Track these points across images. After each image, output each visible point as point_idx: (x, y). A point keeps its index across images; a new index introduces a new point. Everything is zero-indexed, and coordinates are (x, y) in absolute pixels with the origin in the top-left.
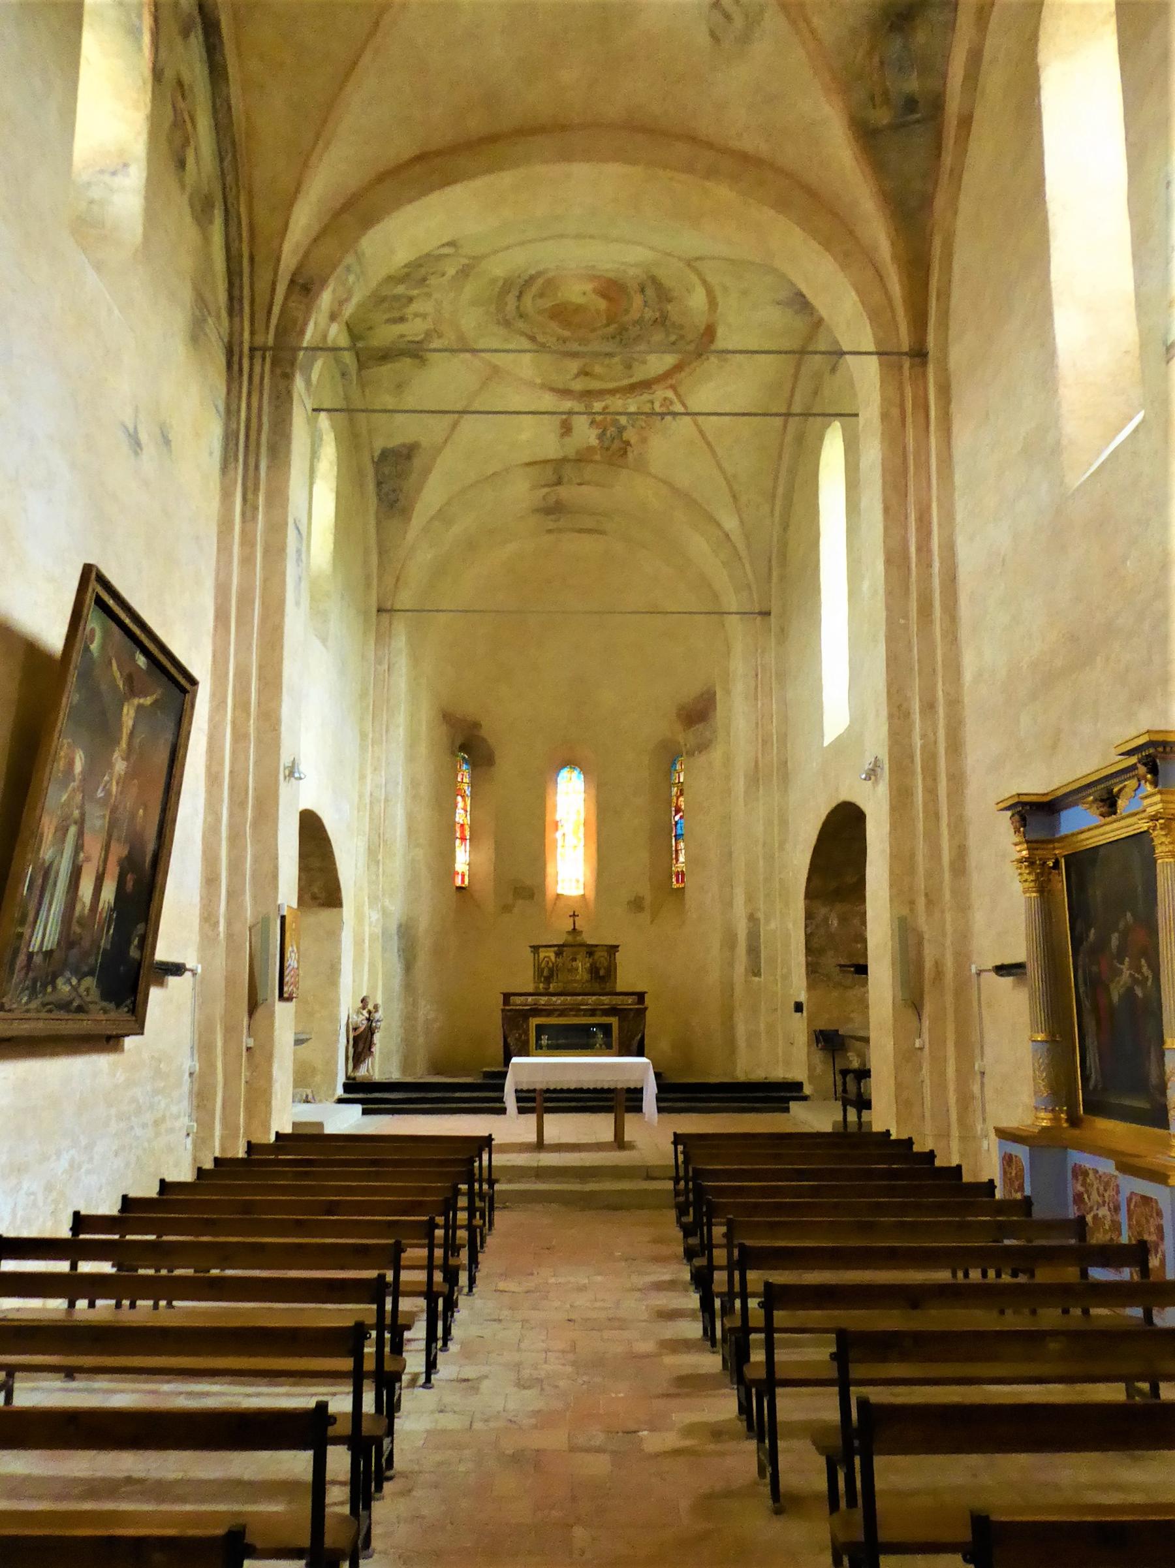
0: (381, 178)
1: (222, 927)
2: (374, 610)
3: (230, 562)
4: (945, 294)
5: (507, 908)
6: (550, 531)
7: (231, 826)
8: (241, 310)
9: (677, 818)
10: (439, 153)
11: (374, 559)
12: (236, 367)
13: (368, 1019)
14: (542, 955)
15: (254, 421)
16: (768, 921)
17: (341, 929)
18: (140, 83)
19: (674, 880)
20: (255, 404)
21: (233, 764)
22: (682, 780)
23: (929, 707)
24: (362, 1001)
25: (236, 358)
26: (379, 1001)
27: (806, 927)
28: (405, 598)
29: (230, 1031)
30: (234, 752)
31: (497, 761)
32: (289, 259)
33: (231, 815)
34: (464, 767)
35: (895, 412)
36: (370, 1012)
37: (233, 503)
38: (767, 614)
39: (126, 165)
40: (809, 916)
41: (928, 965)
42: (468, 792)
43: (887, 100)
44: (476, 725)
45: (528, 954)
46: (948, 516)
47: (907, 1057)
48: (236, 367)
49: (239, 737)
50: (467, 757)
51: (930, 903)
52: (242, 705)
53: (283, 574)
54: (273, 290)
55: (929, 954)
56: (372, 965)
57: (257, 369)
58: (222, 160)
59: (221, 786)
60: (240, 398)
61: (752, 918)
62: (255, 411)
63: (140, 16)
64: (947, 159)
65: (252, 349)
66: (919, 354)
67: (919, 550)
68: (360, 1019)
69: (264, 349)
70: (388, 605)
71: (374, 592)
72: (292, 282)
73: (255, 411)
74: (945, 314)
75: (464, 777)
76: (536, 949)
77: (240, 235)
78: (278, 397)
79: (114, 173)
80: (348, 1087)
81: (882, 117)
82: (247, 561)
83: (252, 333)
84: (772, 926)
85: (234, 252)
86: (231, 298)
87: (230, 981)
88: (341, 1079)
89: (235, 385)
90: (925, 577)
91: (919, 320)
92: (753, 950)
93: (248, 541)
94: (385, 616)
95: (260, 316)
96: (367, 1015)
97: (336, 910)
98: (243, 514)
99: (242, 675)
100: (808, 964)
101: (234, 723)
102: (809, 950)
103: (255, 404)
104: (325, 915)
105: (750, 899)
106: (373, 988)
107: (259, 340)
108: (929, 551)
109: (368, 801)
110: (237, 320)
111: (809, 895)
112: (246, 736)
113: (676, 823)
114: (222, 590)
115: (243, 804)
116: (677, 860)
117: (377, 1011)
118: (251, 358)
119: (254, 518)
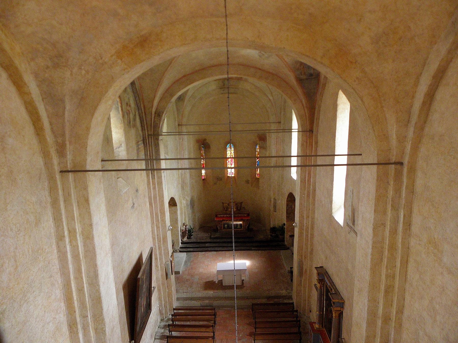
0: (175, 83)
1: (159, 266)
2: (177, 124)
3: (151, 192)
4: (318, 119)
5: (215, 184)
6: (222, 94)
7: (158, 246)
8: (145, 130)
9: (257, 160)
10: (188, 75)
11: (176, 113)
12: (145, 143)
13: (185, 228)
14: (224, 205)
15: (151, 154)
16: (278, 201)
17: (177, 211)
18: (120, 121)
19: (257, 175)
20: (151, 150)
21: (157, 233)
22: (258, 151)
23: (308, 217)
24: (183, 224)
25: (145, 141)
26: (187, 224)
27: (287, 208)
28: (185, 121)
29: (163, 284)
30: (157, 231)
31: (211, 146)
32: (154, 110)
33: (158, 244)
34: (203, 149)
35: (305, 144)
36: (185, 226)
37: (150, 177)
38: (280, 122)
39: (121, 144)
40: (287, 205)
41: (304, 270)
42: (204, 155)
43: (305, 74)
44: (205, 140)
45: (221, 204)
46: (315, 176)
47: (300, 284)
48: (145, 143)
49: (158, 227)
50: (203, 146)
51: (305, 258)
52: (158, 221)
53: (162, 188)
54: (151, 121)
55: (304, 267)
56: (185, 213)
57: (150, 140)
58: (135, 98)
59: (155, 240)
60: (147, 151)
61: (274, 199)
62: (151, 151)
63: (118, 104)
64: (320, 89)
65: (148, 135)
66: (311, 131)
67: (308, 181)
68: (183, 229)
69: (151, 135)
70: (180, 124)
71: (177, 122)
72: (155, 113)
73: (151, 151)
74: (318, 123)
75: (203, 152)
76: (223, 203)
77: (142, 113)
78: (156, 145)
79: (119, 148)
80: (181, 243)
81: (304, 77)
82: (154, 188)
83: (148, 131)
84: (279, 202)
85: (141, 116)
86: (142, 126)
87: (162, 275)
88: (180, 241)
89: (146, 148)
90: (309, 188)
91: (312, 122)
92: (275, 207)
93: (154, 184)
94: (180, 127)
95: (149, 127)
96: (185, 227)
97: (176, 207)
98: (152, 177)
99: (157, 214)
100: (287, 216)
101: (156, 225)
102: (287, 213)
103: (151, 150)
104: (173, 208)
105: (274, 194)
106: (185, 220)
107: (150, 133)
108: (310, 181)
109: (180, 175)
110: (144, 131)
111: (287, 201)
112: (159, 227)
113: (257, 162)
114: (150, 198)
115: (160, 241)
116: (257, 171)
117: (187, 226)
118: (148, 138)
119: (154, 178)
